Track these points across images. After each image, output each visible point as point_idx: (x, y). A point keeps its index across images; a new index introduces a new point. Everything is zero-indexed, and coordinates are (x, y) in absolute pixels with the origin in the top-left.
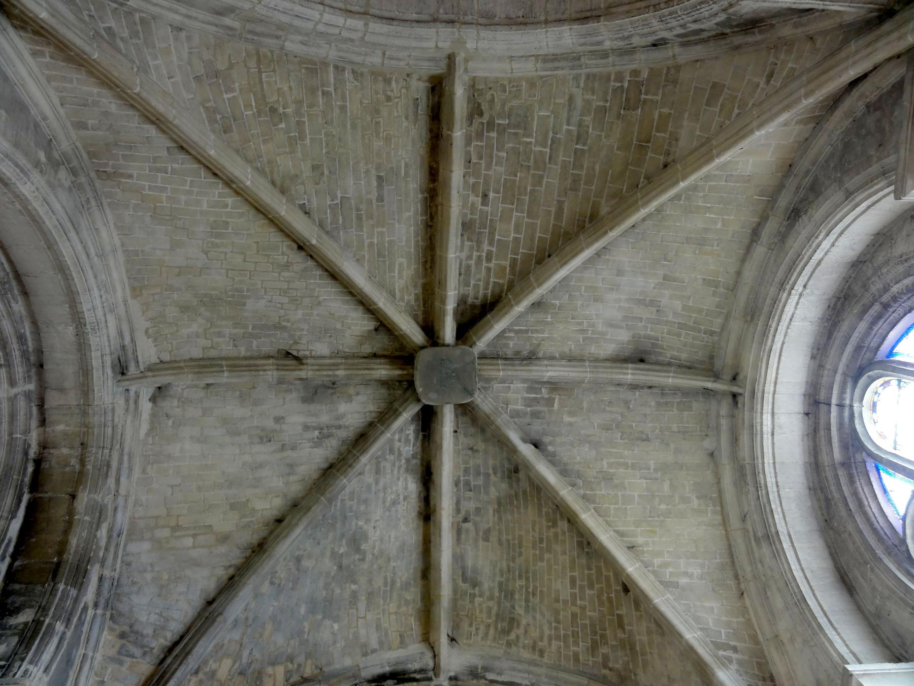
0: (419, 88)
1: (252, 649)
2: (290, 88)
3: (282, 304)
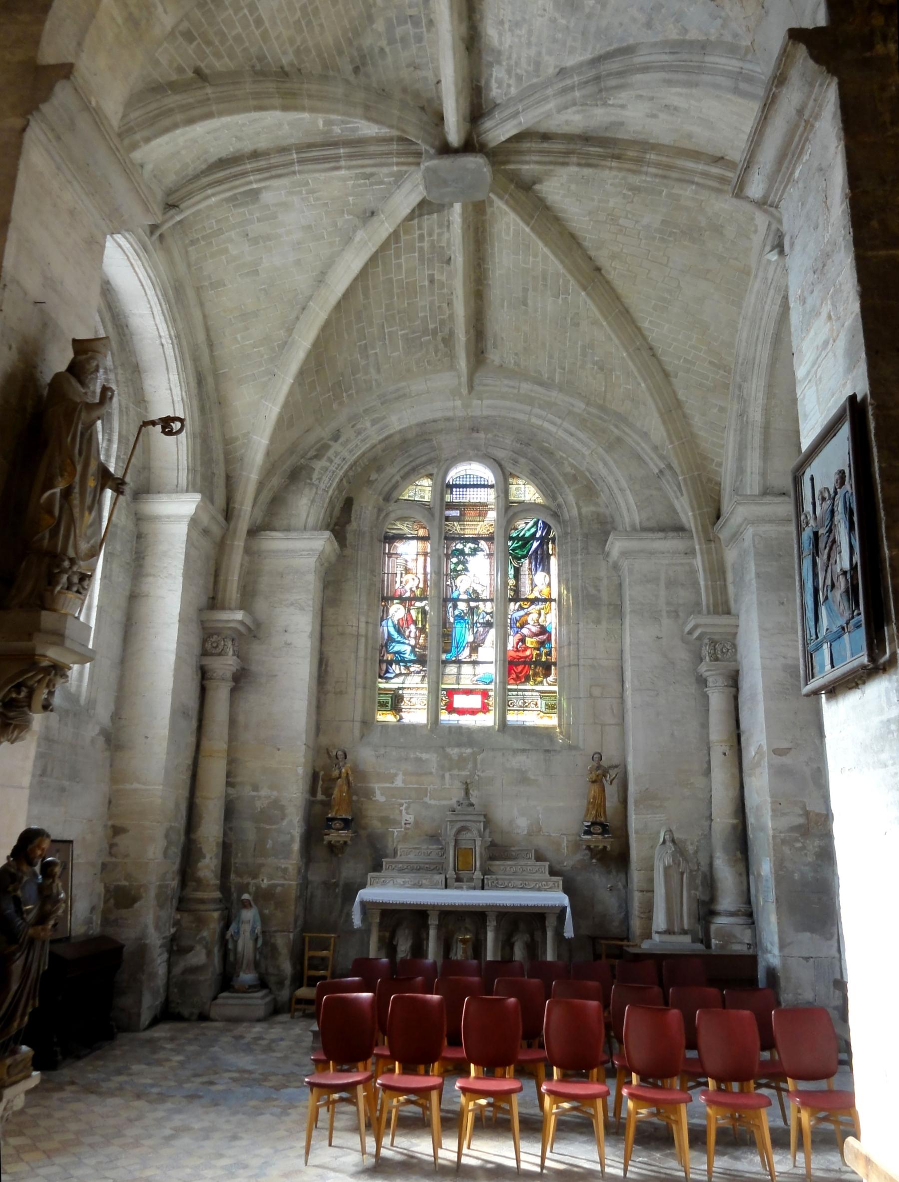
0: (494, 356)
3: (626, 217)
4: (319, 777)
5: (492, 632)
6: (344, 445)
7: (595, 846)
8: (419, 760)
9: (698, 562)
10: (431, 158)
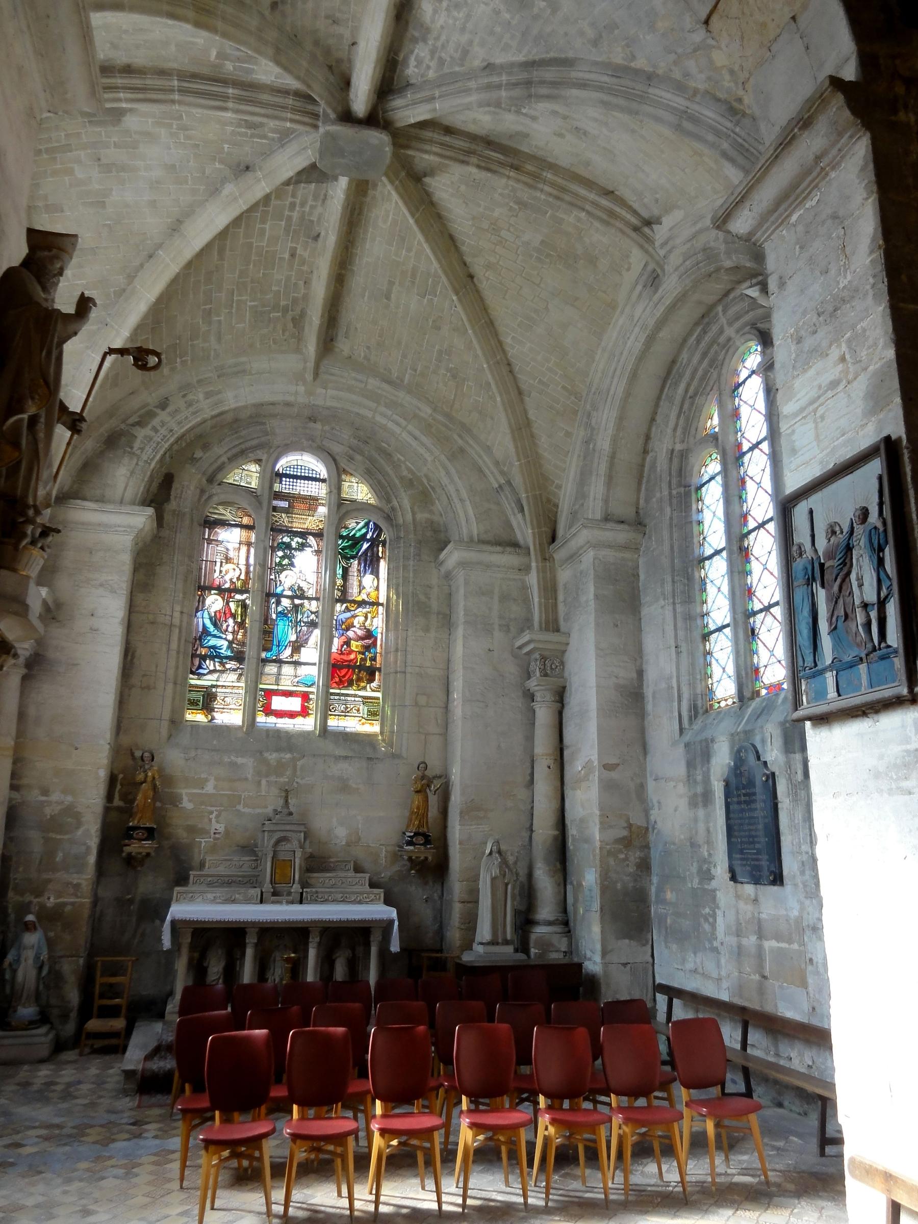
0: (343, 346)
1: (689, 31)
2: (438, 383)
3: (509, 230)
4: (117, 780)
5: (317, 633)
6: (173, 414)
7: (417, 857)
8: (233, 765)
9: (533, 579)
10: (333, 123)
